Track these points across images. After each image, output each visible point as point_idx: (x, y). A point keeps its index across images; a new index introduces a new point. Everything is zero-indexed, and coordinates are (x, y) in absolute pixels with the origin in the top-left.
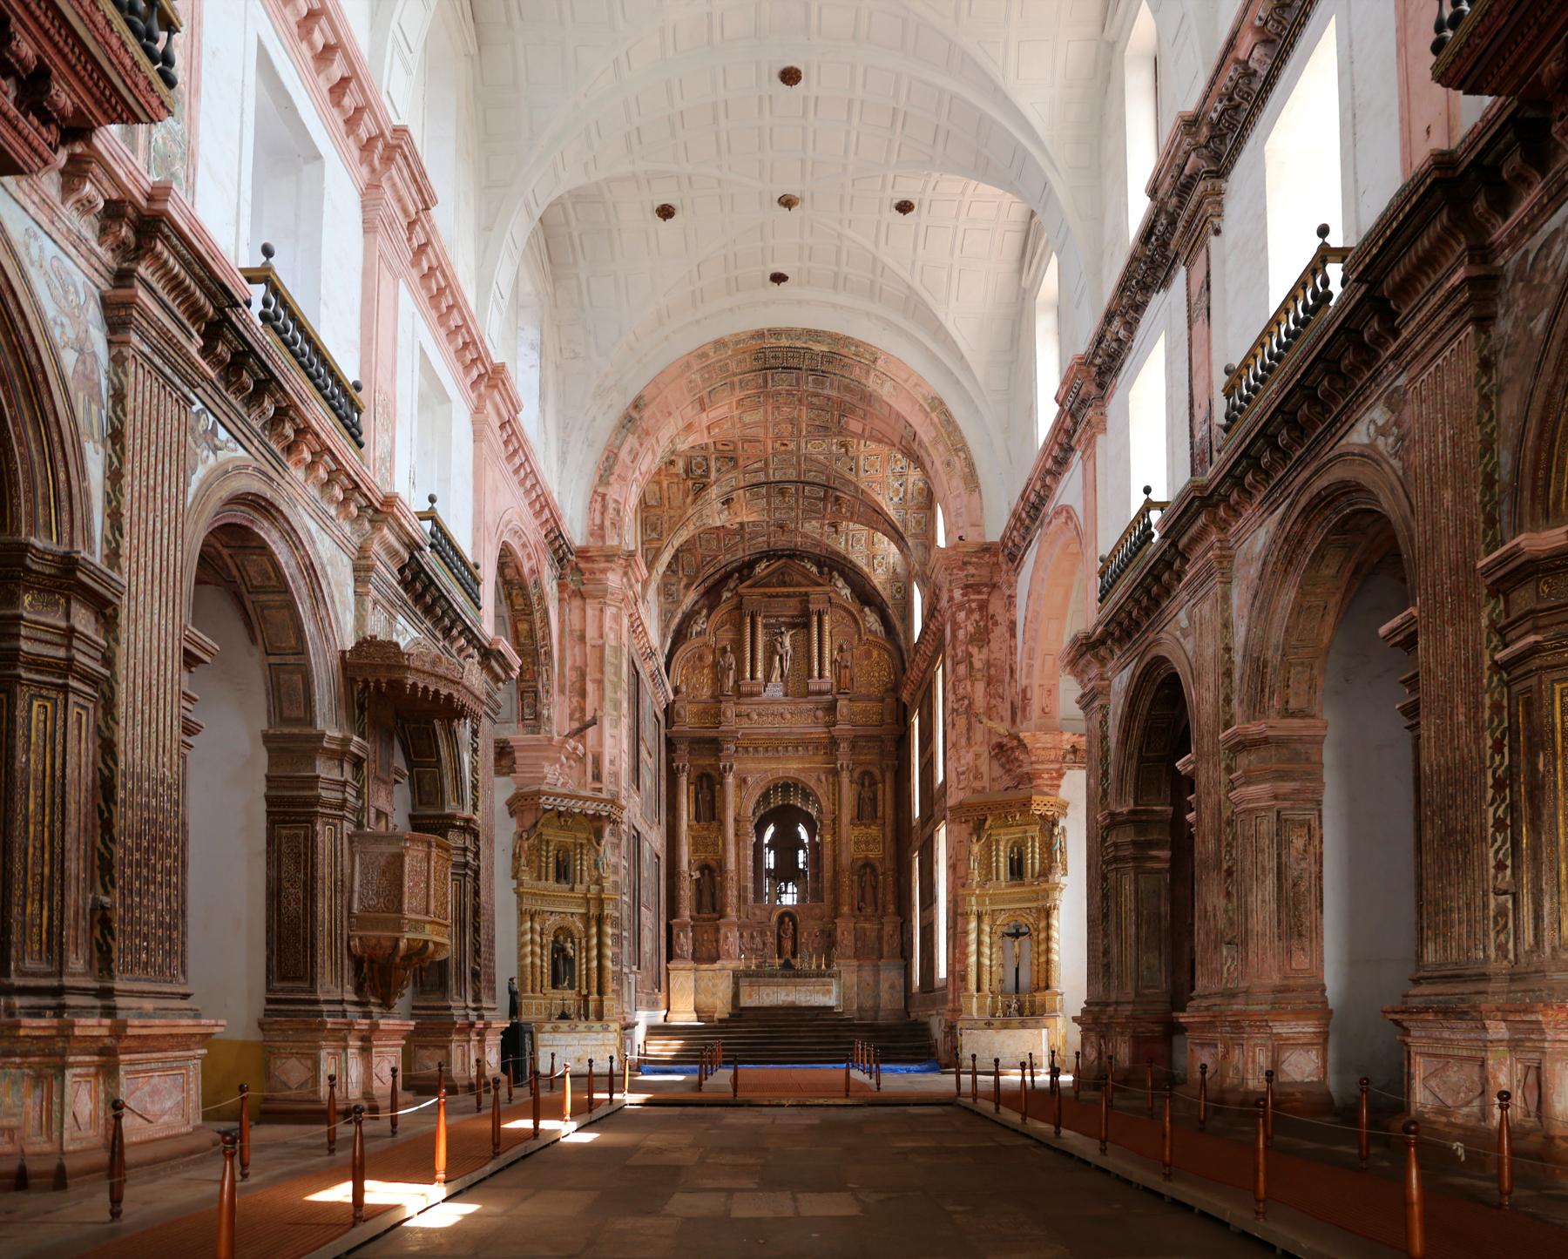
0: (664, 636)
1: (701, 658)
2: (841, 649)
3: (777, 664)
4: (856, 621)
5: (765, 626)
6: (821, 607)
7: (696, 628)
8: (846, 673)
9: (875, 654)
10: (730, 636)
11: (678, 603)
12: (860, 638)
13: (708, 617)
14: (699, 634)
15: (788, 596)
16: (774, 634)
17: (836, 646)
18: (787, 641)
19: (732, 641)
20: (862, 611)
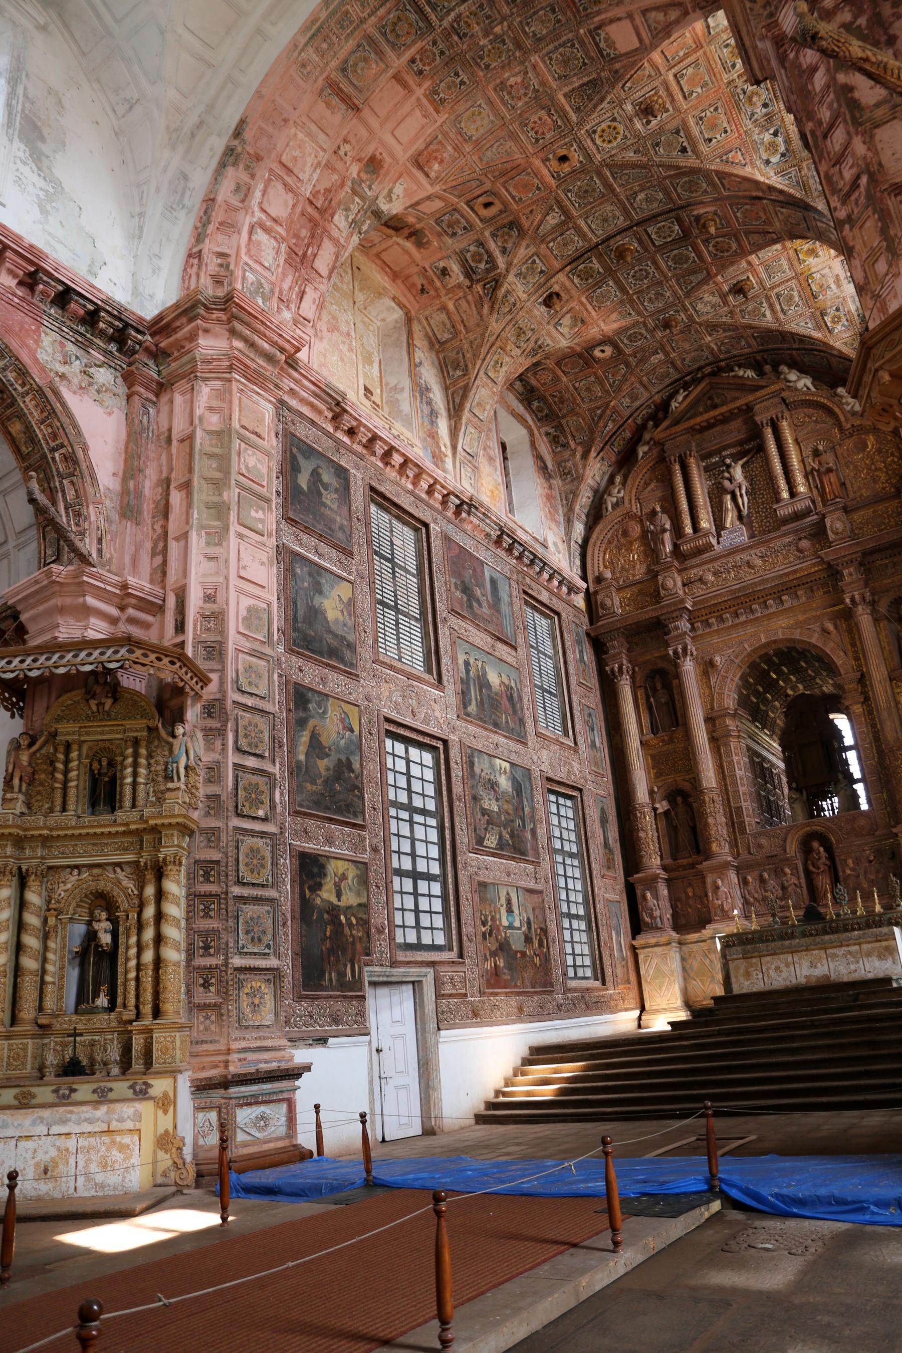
0: (569, 521)
1: (625, 533)
2: (816, 453)
3: (729, 505)
4: (830, 412)
5: (706, 469)
6: (772, 413)
7: (610, 501)
8: (831, 482)
9: (871, 441)
10: (659, 494)
11: (579, 479)
12: (841, 429)
13: (624, 483)
14: (615, 506)
15: (725, 420)
16: (717, 472)
17: (808, 452)
18: (738, 473)
19: (662, 500)
20: (836, 395)
